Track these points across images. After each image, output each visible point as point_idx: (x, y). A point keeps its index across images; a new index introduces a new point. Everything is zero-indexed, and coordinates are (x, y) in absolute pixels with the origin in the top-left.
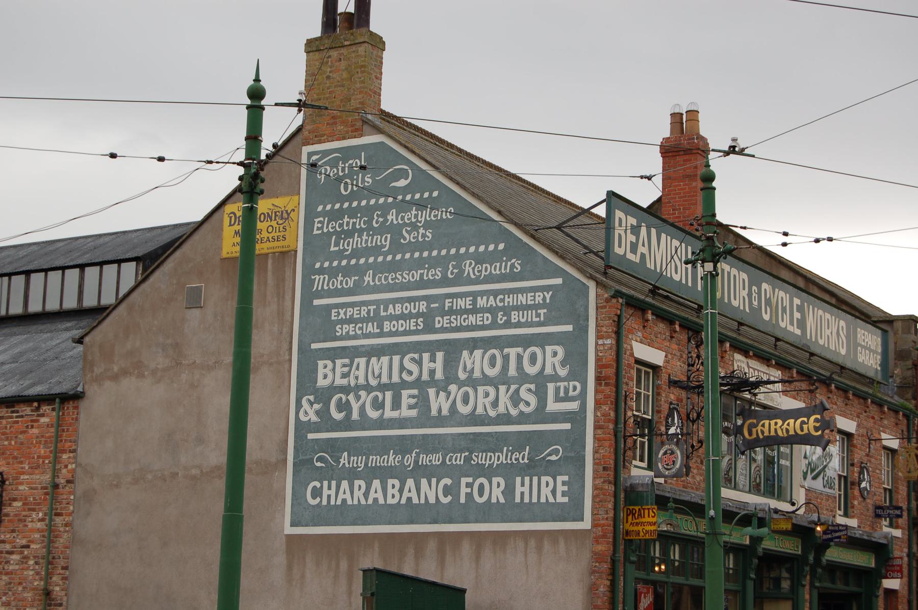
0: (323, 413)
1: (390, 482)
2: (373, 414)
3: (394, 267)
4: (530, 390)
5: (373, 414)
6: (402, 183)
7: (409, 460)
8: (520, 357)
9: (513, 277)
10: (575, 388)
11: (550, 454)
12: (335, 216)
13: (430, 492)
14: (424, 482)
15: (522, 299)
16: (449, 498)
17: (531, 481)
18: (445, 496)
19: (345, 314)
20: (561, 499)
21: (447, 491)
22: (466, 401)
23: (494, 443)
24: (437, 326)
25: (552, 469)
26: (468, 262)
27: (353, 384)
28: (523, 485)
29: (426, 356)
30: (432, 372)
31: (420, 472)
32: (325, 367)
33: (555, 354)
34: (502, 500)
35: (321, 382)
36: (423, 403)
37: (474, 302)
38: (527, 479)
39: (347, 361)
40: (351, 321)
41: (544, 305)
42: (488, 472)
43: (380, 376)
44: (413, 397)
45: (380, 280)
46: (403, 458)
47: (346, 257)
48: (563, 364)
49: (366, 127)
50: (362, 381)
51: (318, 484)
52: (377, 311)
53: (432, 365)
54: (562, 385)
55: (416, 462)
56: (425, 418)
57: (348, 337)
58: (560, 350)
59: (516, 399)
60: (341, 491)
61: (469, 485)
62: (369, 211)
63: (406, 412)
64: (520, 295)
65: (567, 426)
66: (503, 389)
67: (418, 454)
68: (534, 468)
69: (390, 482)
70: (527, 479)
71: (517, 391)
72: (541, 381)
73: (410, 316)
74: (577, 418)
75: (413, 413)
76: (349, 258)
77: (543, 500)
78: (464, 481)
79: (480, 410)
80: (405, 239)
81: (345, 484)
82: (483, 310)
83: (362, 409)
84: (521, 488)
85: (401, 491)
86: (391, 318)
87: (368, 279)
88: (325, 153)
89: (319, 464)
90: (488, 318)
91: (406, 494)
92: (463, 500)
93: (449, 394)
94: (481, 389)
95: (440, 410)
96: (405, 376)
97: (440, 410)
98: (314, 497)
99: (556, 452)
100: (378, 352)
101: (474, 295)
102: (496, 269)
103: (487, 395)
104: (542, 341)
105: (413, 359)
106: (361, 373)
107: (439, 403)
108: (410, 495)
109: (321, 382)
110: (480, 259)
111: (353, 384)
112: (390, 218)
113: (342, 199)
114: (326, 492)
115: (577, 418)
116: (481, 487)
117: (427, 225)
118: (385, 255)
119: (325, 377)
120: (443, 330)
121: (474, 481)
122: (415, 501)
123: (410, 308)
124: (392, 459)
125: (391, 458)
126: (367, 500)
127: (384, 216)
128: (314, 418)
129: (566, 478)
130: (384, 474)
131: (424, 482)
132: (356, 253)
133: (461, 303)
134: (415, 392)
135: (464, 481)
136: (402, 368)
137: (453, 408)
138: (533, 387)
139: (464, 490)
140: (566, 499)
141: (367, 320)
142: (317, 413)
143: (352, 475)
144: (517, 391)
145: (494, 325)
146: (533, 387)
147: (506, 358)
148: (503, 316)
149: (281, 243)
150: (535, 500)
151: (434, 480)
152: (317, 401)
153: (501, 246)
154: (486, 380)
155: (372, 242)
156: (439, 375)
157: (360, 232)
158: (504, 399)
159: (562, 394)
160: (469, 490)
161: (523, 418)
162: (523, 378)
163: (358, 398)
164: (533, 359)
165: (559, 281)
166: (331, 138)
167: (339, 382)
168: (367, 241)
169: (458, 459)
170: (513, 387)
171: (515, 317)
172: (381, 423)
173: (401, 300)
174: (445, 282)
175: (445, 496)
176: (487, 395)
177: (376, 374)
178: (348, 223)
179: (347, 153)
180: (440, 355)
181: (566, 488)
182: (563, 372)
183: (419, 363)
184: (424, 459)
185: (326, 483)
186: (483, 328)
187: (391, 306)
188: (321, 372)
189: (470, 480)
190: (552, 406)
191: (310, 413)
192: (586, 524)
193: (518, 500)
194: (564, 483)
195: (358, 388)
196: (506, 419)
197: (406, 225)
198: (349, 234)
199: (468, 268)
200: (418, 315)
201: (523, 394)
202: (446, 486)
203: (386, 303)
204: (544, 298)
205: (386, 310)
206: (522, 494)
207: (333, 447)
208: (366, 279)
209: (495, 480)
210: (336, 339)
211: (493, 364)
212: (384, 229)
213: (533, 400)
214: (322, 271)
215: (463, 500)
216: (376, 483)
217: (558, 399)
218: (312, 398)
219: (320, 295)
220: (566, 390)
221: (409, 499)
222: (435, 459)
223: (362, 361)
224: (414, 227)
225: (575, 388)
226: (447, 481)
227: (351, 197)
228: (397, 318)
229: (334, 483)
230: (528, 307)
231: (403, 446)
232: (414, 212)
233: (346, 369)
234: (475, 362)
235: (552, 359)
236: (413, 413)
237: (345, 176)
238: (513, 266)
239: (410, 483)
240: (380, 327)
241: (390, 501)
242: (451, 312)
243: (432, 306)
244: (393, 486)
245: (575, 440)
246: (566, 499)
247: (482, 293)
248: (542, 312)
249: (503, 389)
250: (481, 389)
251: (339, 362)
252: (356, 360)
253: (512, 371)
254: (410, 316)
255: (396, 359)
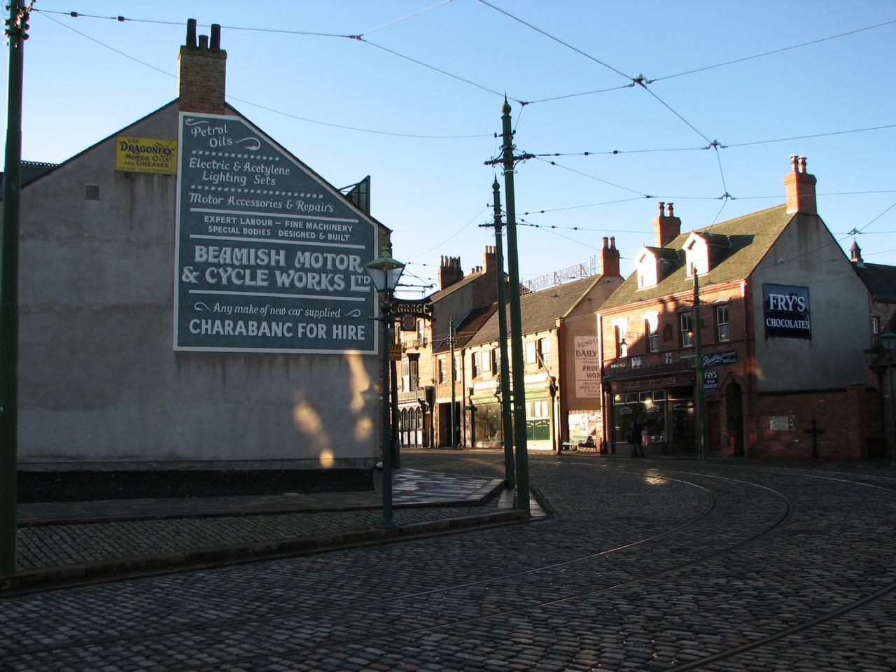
0: (201, 278)
1: (251, 323)
2: (238, 282)
3: (249, 196)
4: (340, 278)
5: (238, 282)
6: (254, 148)
7: (264, 311)
8: (334, 260)
9: (327, 214)
10: (367, 280)
11: (353, 314)
12: (204, 159)
13: (278, 330)
14: (274, 324)
15: (334, 227)
16: (291, 334)
17: (342, 327)
18: (289, 333)
19: (215, 219)
20: (360, 338)
21: (289, 330)
22: (300, 279)
23: (321, 305)
24: (280, 235)
25: (355, 322)
26: (300, 202)
27: (222, 262)
28: (337, 329)
29: (273, 252)
30: (278, 262)
31: (270, 318)
32: (201, 250)
33: (355, 260)
34: (325, 337)
35: (198, 259)
36: (271, 278)
37: (304, 225)
38: (340, 327)
39: (217, 248)
40: (219, 224)
41: (348, 232)
42: (317, 321)
43: (241, 260)
44: (265, 274)
45: (239, 202)
46: (259, 309)
47: (214, 185)
48: (360, 266)
49: (226, 110)
50: (228, 261)
51: (198, 321)
52: (238, 221)
53: (277, 257)
54: (360, 277)
55: (268, 312)
56: (273, 286)
57: (217, 234)
58: (358, 260)
59: (332, 282)
60: (216, 326)
61: (303, 327)
62: (231, 161)
63: (259, 283)
64: (333, 226)
65: (363, 299)
66: (323, 276)
67: (269, 308)
68: (344, 321)
69: (251, 323)
70: (340, 327)
71: (333, 278)
72: (347, 274)
73: (261, 227)
74: (369, 296)
75: (266, 284)
76: (217, 186)
77: (350, 338)
78: (300, 325)
79: (309, 286)
80: (257, 182)
81: (218, 322)
82: (310, 230)
83: (229, 278)
84: (337, 331)
85: (258, 328)
86: (248, 226)
87: (231, 200)
88: (197, 119)
89: (198, 309)
90: (313, 235)
91: (261, 331)
92: (300, 335)
93: (289, 275)
94: (310, 275)
95: (283, 284)
96: (258, 261)
97: (283, 284)
98: (195, 329)
99: (357, 313)
100: (241, 245)
101: (305, 221)
102: (318, 208)
103: (314, 278)
104: (348, 252)
105: (264, 252)
106: (228, 257)
107: (282, 279)
108: (264, 331)
109: (198, 259)
110: (307, 201)
111: (222, 262)
112: (246, 167)
113: (211, 150)
114: (204, 326)
115: (369, 296)
116: (312, 330)
117: (272, 176)
118: (243, 188)
119: (201, 256)
120: (284, 238)
121: (307, 325)
122: (268, 334)
123: (259, 222)
124: (251, 310)
125: (251, 309)
126: (234, 332)
127: (242, 165)
128: (194, 281)
129: (363, 327)
130: (246, 318)
131: (274, 324)
132: (222, 184)
133: (296, 224)
134: (266, 272)
135: (300, 325)
136: (257, 257)
137: (292, 282)
138: (342, 276)
139: (300, 330)
140: (363, 338)
141: (231, 225)
142: (196, 277)
143: (223, 317)
144: (333, 278)
145: (317, 239)
146: (342, 276)
147: (325, 259)
148: (323, 235)
149: (165, 169)
150: (345, 338)
151: (281, 324)
152: (195, 270)
153: (321, 196)
154: (312, 270)
155: (233, 179)
156: (282, 263)
157: (225, 172)
158: (325, 281)
159: (360, 282)
160: (304, 330)
161: (336, 293)
162: (335, 271)
163: (226, 271)
164: (342, 261)
165: (357, 221)
166: (202, 110)
167: (211, 260)
168: (229, 178)
169: (297, 313)
170: (330, 276)
171: (330, 236)
172: (243, 288)
173: (256, 217)
174: (284, 210)
175: (289, 333)
176: (314, 278)
177: (239, 258)
178: (215, 165)
179: (214, 123)
180: (282, 253)
181: (363, 332)
182: (360, 270)
183: (269, 255)
184: (274, 311)
185: (204, 321)
186: (310, 240)
187: (248, 220)
188: (198, 253)
189: (305, 325)
190: (353, 288)
191: (190, 277)
192: (375, 352)
193: (334, 337)
194: (362, 330)
195: (225, 266)
196: (326, 292)
197: (256, 173)
198: (217, 172)
199: (300, 205)
200: (267, 227)
201: (336, 279)
202: (288, 327)
203: (245, 217)
204: (348, 229)
205: (244, 221)
206: (337, 334)
207: (210, 300)
208: (230, 200)
209: (320, 326)
210: (209, 234)
211: (317, 260)
212: (241, 173)
213: (343, 284)
214: (196, 191)
215: (300, 335)
216: (241, 323)
217: (357, 284)
218: (191, 268)
219: (197, 205)
220: (362, 280)
221: (264, 333)
222: (282, 312)
223: (229, 250)
224: (263, 176)
225: (367, 280)
226: (290, 325)
227: (218, 149)
228: (252, 227)
229: (210, 321)
230: (338, 233)
231: (259, 302)
232: (262, 167)
233: (217, 253)
234: (307, 258)
235: (354, 262)
236: (266, 284)
237: (212, 136)
238: (328, 208)
239: (264, 324)
240: (241, 230)
241: (250, 334)
242: (289, 228)
243: (277, 223)
244: (253, 325)
245: (368, 307)
246: (363, 338)
247: (309, 221)
248: (347, 236)
249: (323, 276)
250: (310, 275)
251: (211, 249)
252: (224, 249)
253: (329, 266)
254: (261, 227)
255: (252, 251)
